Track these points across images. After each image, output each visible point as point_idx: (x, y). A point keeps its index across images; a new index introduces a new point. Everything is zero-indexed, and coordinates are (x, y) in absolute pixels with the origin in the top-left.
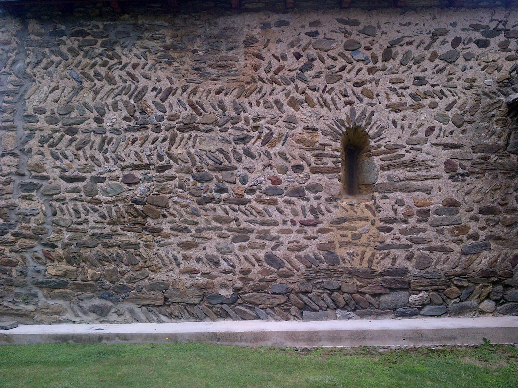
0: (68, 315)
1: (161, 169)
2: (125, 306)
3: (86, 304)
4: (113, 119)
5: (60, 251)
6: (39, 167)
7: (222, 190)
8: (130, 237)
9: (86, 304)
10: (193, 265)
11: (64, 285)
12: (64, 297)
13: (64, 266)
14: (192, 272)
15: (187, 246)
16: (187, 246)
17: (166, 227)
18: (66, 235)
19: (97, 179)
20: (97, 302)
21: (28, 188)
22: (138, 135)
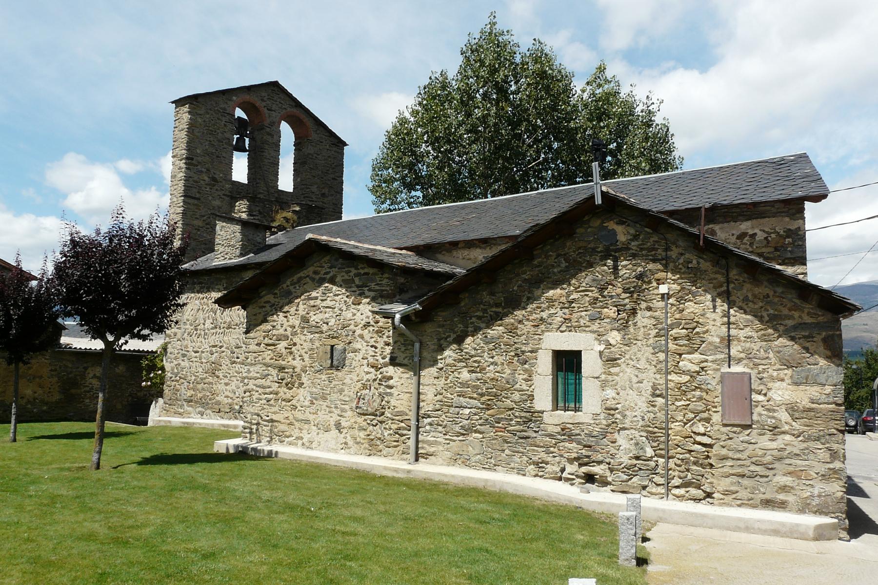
0: (192, 415)
1: (221, 347)
2: (209, 411)
3: (198, 410)
4: (208, 324)
5: (191, 385)
6: (186, 347)
7: (238, 358)
8: (210, 379)
9: (198, 410)
10: (227, 393)
11: (191, 401)
12: (191, 406)
13: (192, 392)
14: (227, 397)
15: (226, 384)
16: (226, 384)
17: (221, 375)
18: (193, 378)
19: (203, 352)
20: (200, 409)
21: (184, 356)
22: (214, 331)
